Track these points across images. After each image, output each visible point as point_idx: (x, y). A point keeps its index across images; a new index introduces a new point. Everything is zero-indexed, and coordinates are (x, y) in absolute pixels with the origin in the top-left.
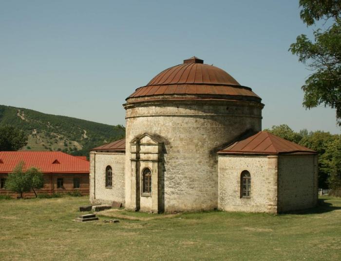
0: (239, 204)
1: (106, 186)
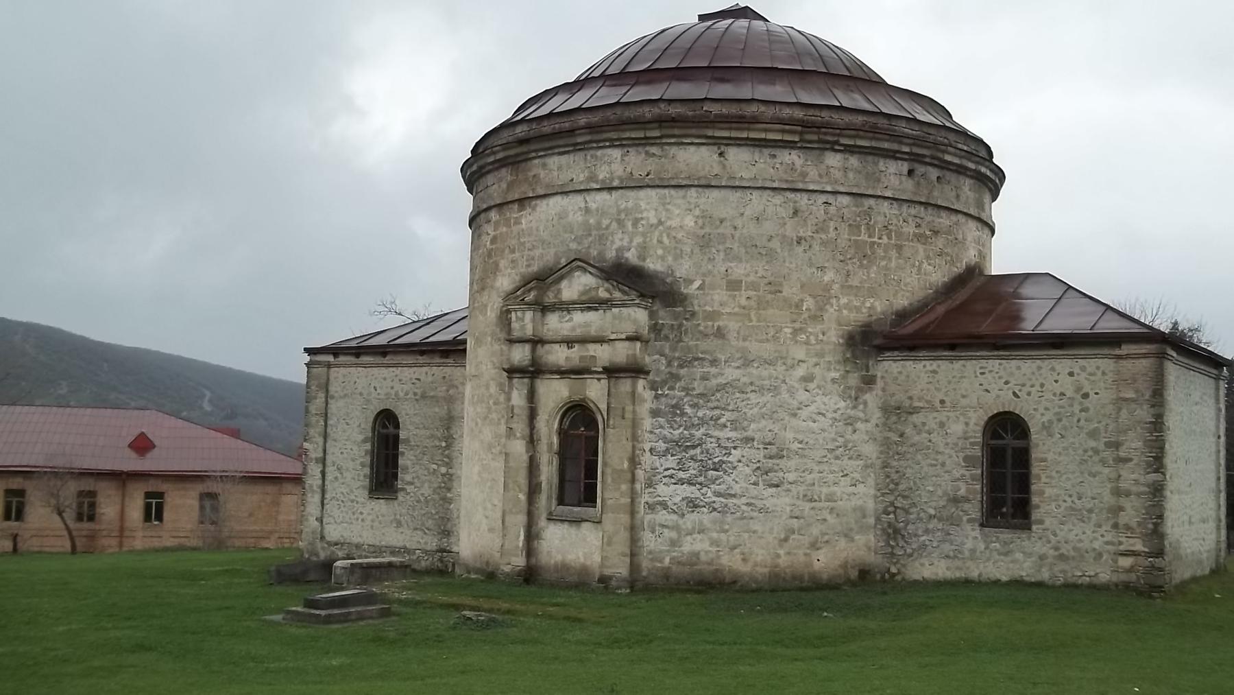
0: (973, 551)
1: (371, 491)
